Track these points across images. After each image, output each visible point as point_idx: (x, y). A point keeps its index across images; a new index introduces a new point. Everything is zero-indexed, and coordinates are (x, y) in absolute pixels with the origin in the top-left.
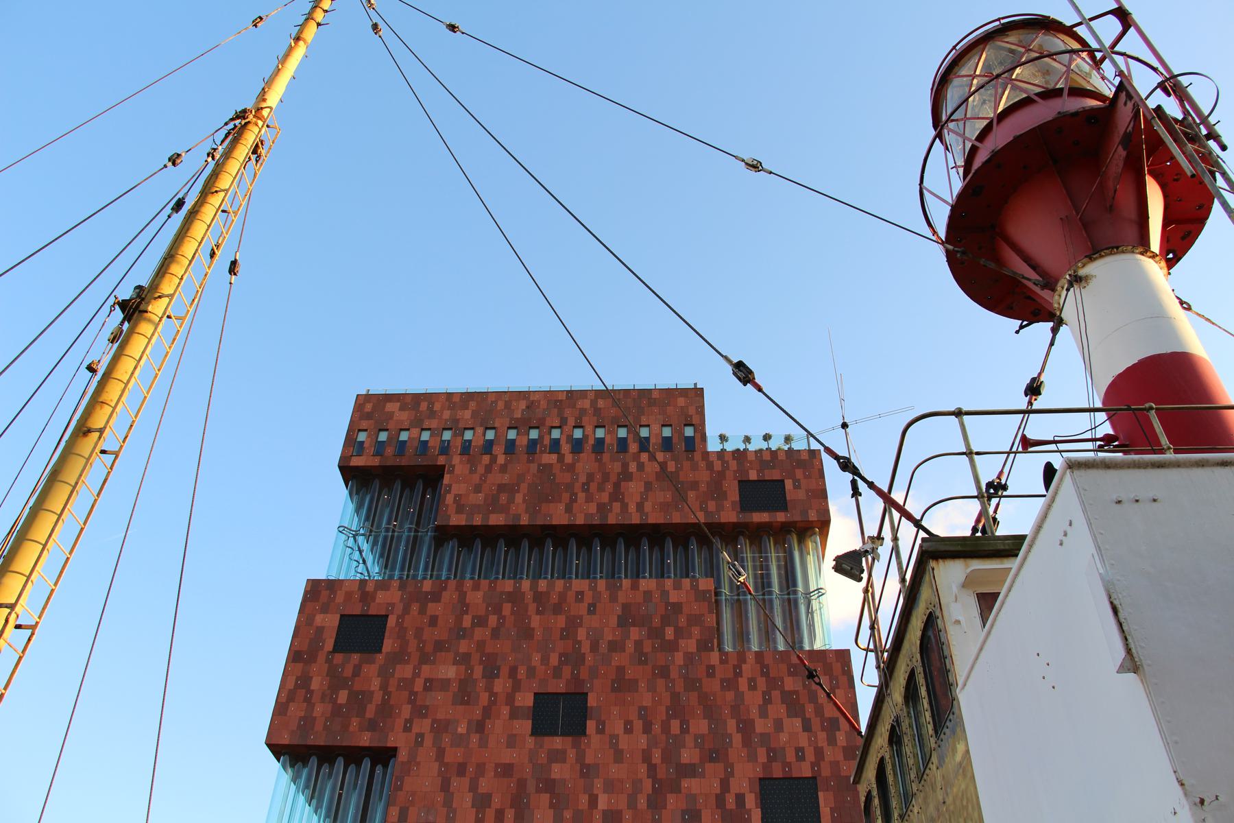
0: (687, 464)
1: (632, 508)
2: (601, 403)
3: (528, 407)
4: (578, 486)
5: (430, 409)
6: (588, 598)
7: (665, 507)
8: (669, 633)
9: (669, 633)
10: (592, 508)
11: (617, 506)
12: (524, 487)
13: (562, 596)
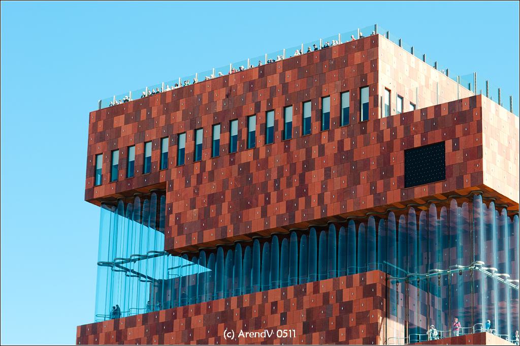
0: (360, 138)
1: (314, 201)
2: (289, 75)
3: (227, 96)
4: (271, 183)
5: (149, 116)
6: (281, 309)
7: (342, 195)
8: (342, 333)
9: (342, 333)
10: (282, 209)
11: (302, 200)
12: (228, 194)
13: (261, 308)
